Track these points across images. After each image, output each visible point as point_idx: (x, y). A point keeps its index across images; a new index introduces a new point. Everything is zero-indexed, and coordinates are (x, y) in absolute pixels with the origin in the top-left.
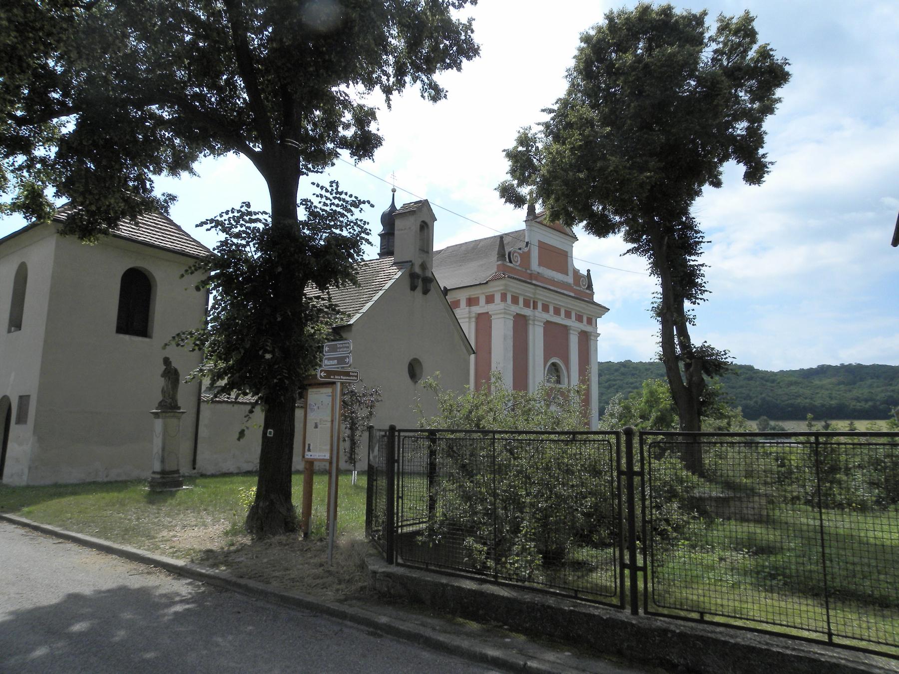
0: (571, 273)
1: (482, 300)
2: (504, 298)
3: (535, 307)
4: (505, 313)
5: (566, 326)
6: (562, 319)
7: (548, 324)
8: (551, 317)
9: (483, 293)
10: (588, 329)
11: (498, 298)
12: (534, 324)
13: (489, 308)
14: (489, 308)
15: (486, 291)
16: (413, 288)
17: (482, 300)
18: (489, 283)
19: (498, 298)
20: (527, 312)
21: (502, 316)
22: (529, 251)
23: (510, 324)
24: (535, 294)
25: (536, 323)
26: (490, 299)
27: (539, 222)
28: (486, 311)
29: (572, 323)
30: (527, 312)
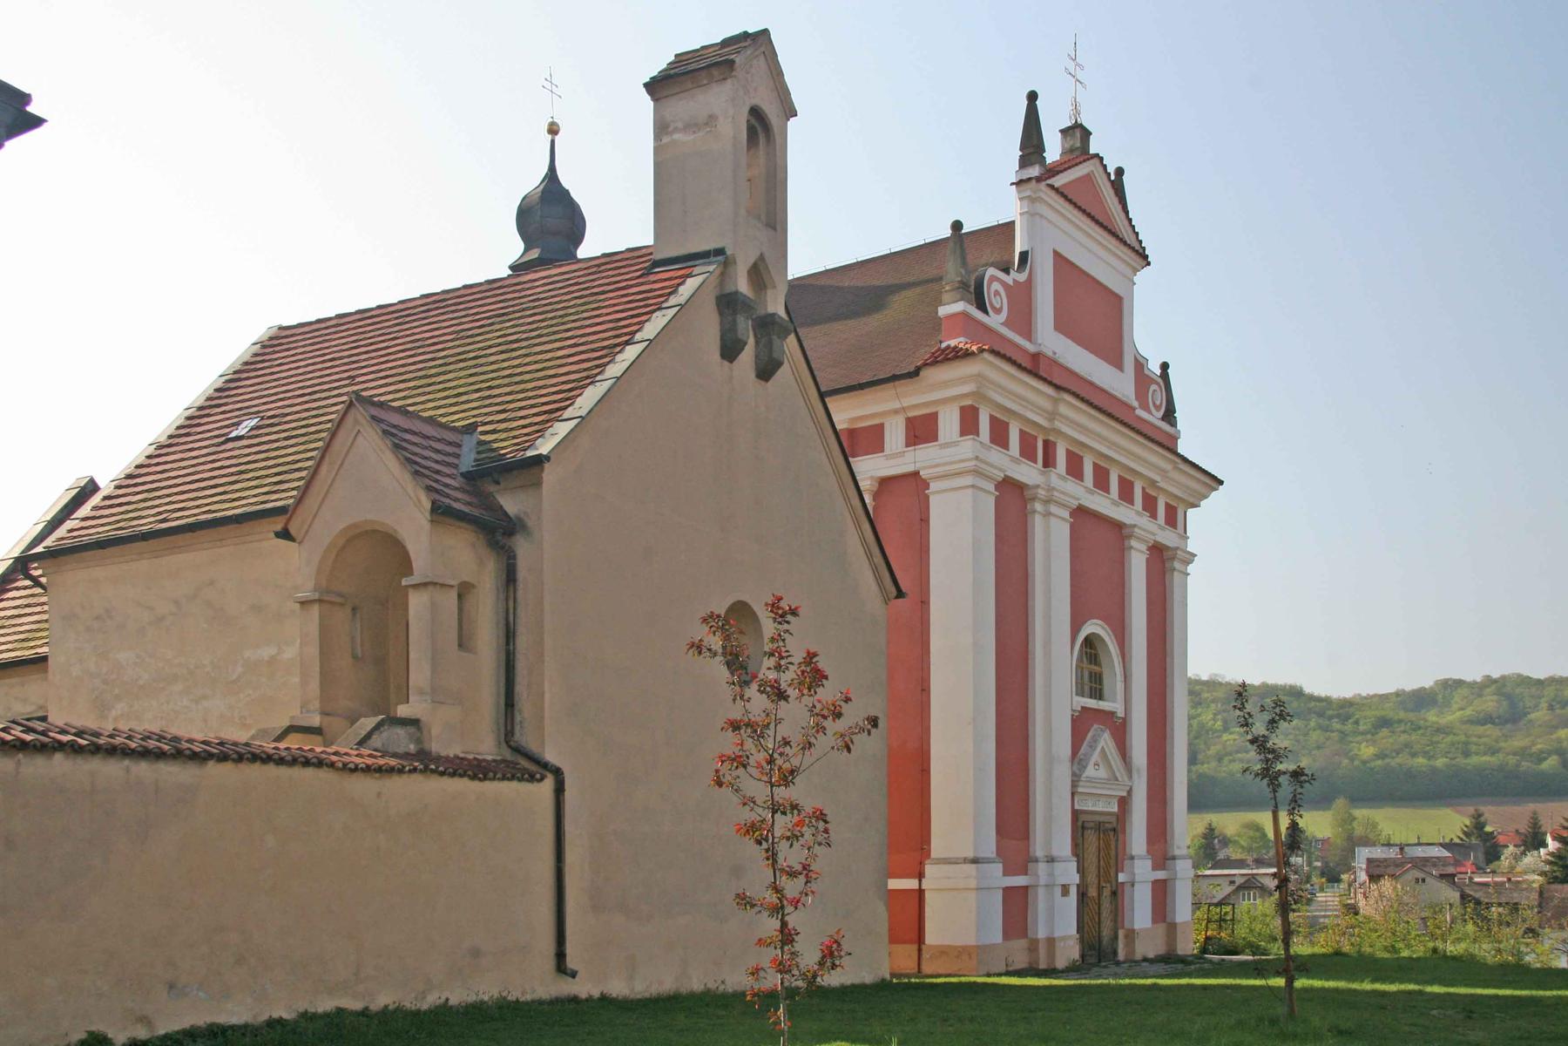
1: (895, 435)
2: (969, 424)
3: (1049, 462)
4: (977, 472)
5: (1118, 526)
6: (1114, 503)
7: (1081, 514)
8: (1082, 493)
9: (896, 412)
10: (1167, 538)
11: (949, 423)
12: (1048, 514)
13: (922, 459)
14: (922, 459)
15: (907, 402)
17: (895, 435)
18: (924, 373)
19: (949, 423)
20: (1028, 473)
21: (968, 480)
22: (1030, 280)
23: (989, 503)
24: (1052, 415)
25: (1053, 509)
26: (921, 430)
27: (1056, 190)
28: (910, 468)
30: (1028, 473)
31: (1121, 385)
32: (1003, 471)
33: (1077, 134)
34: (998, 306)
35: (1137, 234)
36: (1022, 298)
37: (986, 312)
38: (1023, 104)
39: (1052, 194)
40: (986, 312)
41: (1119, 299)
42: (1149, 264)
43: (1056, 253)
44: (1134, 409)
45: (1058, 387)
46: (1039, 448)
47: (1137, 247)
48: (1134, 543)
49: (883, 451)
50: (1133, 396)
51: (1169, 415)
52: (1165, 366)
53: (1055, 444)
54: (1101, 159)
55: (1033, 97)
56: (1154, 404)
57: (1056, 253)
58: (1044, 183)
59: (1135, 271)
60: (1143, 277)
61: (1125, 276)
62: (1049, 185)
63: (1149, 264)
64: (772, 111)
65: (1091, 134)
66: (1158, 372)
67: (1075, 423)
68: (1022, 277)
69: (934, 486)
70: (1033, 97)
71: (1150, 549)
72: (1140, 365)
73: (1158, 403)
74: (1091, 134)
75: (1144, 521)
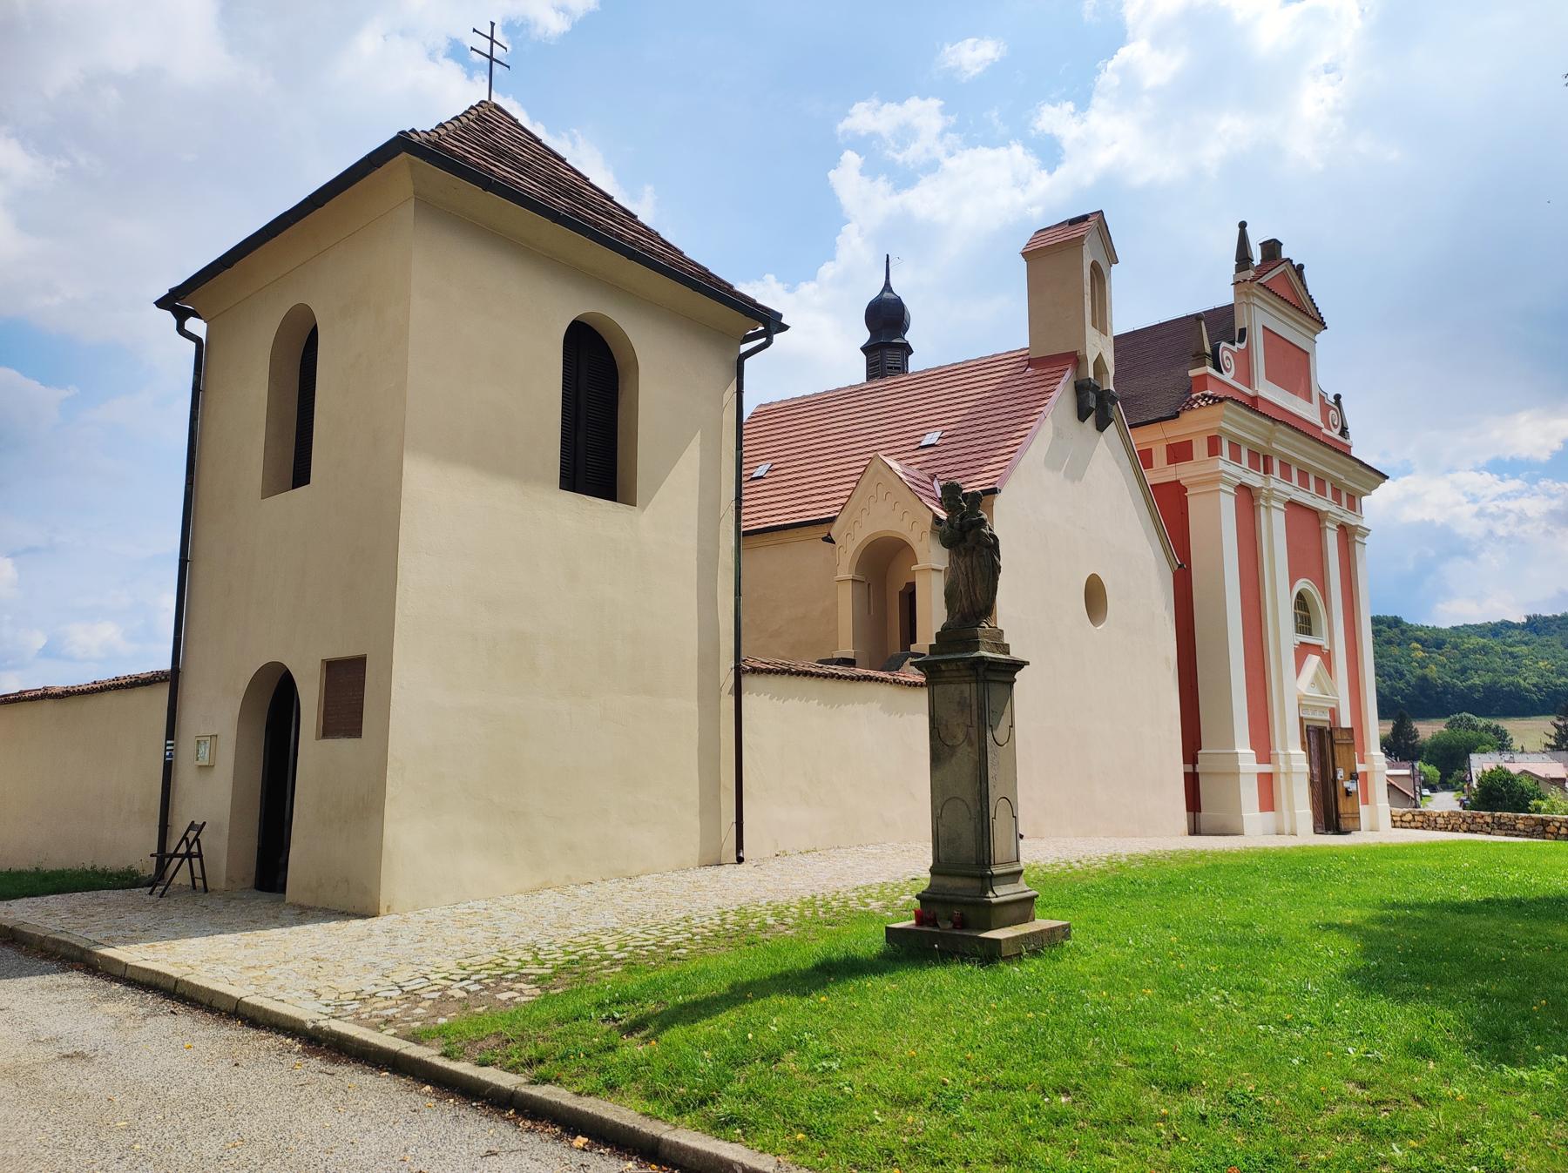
0: (1316, 398)
5: (1315, 512)
6: (1314, 497)
7: (1292, 504)
10: (1350, 519)
11: (1200, 449)
16: (1082, 415)
20: (1254, 479)
28: (1173, 479)
29: (1323, 504)
30: (1254, 479)
31: (1309, 412)
32: (1240, 479)
33: (1272, 248)
34: (1229, 367)
35: (1317, 309)
36: (1245, 358)
37: (1222, 372)
38: (1238, 230)
39: (1261, 289)
40: (1222, 372)
41: (1307, 353)
42: (1326, 328)
43: (1264, 327)
44: (1321, 429)
45: (1274, 420)
46: (1261, 460)
47: (1317, 317)
48: (1328, 524)
49: (1152, 467)
50: (1320, 420)
51: (1344, 432)
52: (1337, 397)
53: (1271, 457)
54: (1291, 261)
55: (1243, 225)
56: (1333, 424)
57: (1264, 327)
58: (1255, 282)
59: (1316, 334)
60: (1321, 337)
61: (1310, 338)
62: (1259, 283)
63: (1326, 328)
64: (1103, 264)
65: (1282, 244)
66: (1333, 401)
67: (1284, 444)
68: (1243, 346)
69: (1190, 492)
70: (1243, 225)
71: (1338, 527)
72: (1322, 398)
73: (1336, 423)
74: (1282, 244)
75: (1333, 508)
